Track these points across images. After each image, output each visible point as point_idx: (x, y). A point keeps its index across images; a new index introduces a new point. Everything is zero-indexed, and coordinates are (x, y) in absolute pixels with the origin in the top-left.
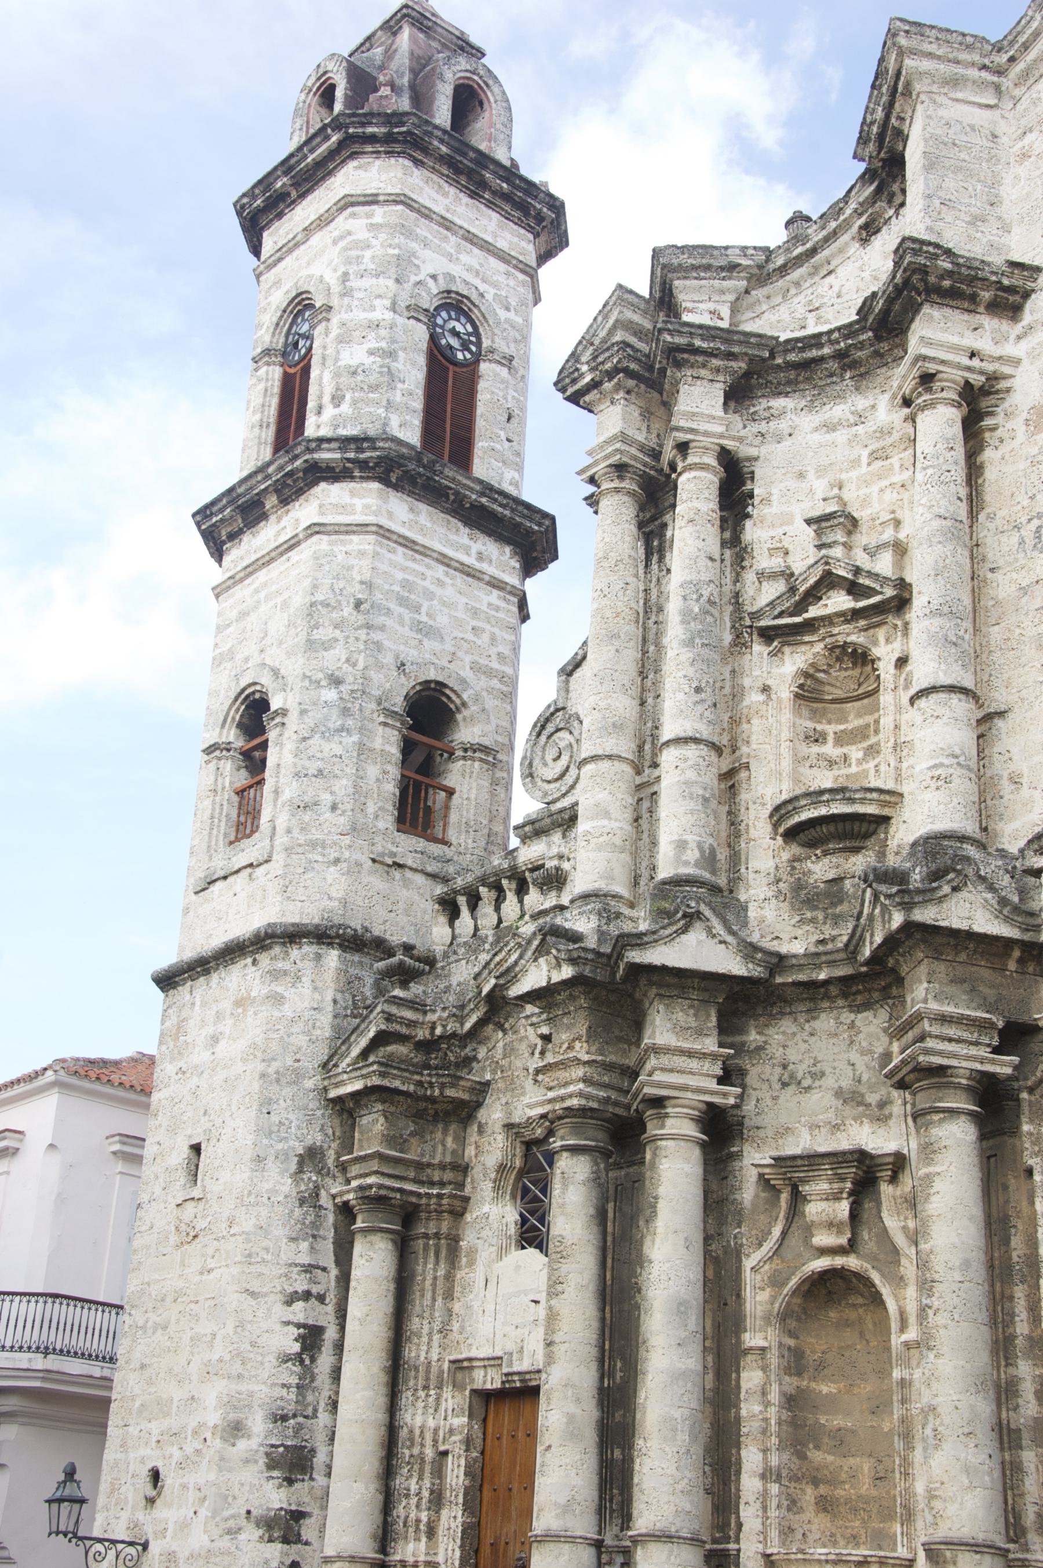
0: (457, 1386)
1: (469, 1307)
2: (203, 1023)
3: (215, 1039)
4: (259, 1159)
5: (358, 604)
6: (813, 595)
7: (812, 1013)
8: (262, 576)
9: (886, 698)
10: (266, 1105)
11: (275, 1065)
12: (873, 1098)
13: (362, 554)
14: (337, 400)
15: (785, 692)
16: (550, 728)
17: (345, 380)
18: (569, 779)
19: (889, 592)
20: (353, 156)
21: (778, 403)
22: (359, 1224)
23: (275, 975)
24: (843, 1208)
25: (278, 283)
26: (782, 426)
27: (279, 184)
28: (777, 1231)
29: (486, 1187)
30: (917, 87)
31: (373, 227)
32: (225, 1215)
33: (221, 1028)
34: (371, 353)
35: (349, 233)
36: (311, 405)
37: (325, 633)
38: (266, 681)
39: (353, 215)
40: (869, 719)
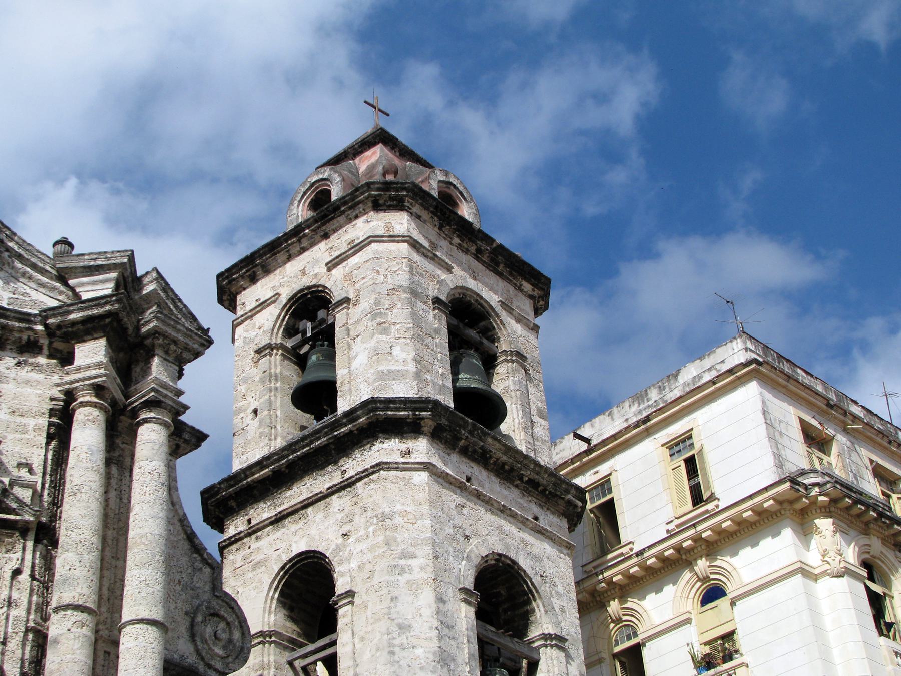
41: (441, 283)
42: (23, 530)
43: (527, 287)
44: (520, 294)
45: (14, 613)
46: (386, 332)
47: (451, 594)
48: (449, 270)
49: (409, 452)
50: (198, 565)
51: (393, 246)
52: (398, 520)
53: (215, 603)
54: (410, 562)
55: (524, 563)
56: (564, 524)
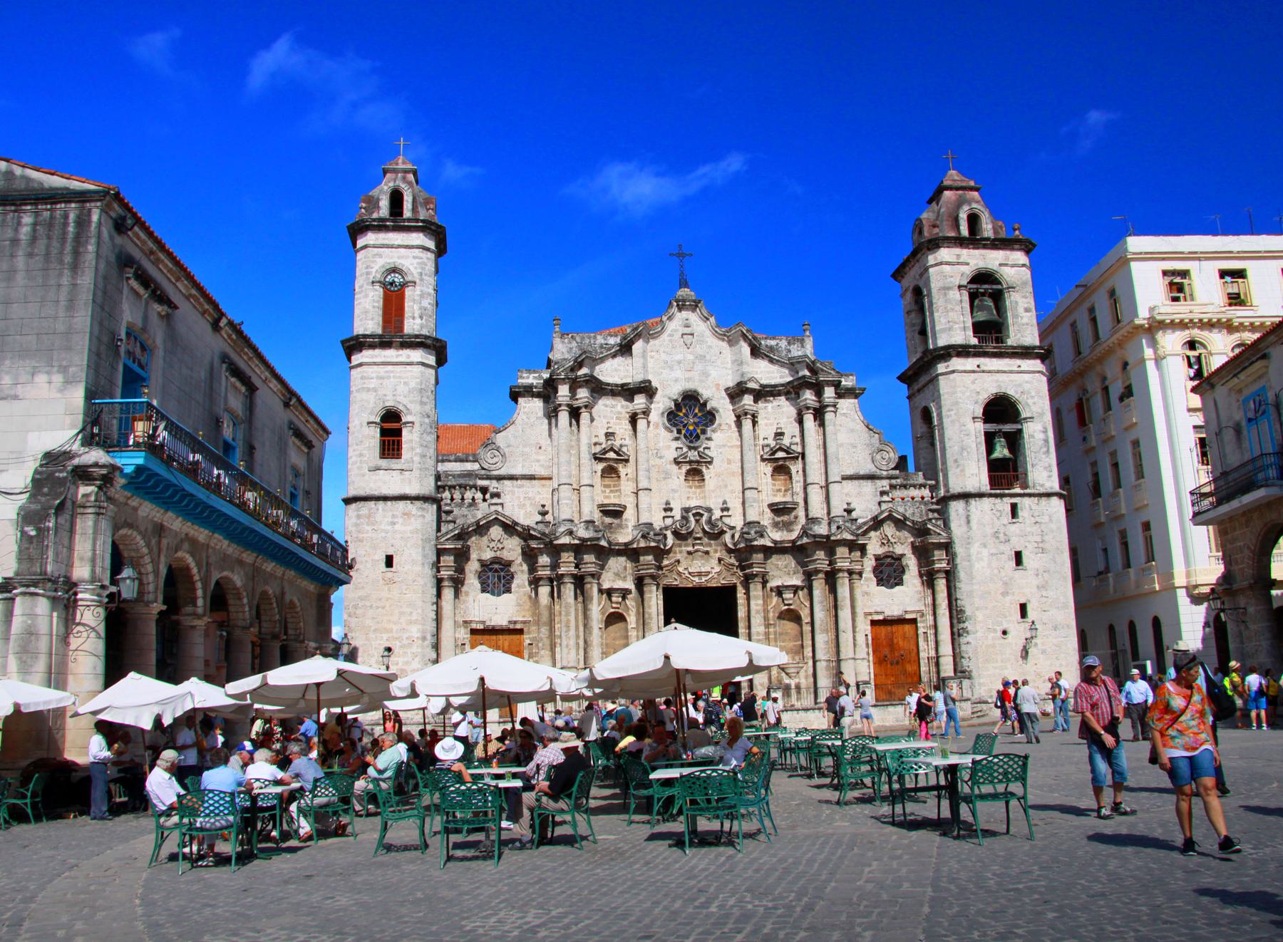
0: (466, 627)
2: (384, 516)
3: (393, 524)
4: (423, 564)
8: (390, 368)
9: (622, 482)
10: (423, 548)
15: (599, 473)
16: (490, 447)
22: (446, 583)
23: (423, 509)
24: (620, 599)
25: (380, 256)
37: (425, 399)
38: (401, 408)
43: (1017, 247)
48: (967, 264)
51: (937, 268)
52: (946, 396)
53: (881, 447)
54: (952, 413)
55: (1011, 392)
56: (1038, 361)
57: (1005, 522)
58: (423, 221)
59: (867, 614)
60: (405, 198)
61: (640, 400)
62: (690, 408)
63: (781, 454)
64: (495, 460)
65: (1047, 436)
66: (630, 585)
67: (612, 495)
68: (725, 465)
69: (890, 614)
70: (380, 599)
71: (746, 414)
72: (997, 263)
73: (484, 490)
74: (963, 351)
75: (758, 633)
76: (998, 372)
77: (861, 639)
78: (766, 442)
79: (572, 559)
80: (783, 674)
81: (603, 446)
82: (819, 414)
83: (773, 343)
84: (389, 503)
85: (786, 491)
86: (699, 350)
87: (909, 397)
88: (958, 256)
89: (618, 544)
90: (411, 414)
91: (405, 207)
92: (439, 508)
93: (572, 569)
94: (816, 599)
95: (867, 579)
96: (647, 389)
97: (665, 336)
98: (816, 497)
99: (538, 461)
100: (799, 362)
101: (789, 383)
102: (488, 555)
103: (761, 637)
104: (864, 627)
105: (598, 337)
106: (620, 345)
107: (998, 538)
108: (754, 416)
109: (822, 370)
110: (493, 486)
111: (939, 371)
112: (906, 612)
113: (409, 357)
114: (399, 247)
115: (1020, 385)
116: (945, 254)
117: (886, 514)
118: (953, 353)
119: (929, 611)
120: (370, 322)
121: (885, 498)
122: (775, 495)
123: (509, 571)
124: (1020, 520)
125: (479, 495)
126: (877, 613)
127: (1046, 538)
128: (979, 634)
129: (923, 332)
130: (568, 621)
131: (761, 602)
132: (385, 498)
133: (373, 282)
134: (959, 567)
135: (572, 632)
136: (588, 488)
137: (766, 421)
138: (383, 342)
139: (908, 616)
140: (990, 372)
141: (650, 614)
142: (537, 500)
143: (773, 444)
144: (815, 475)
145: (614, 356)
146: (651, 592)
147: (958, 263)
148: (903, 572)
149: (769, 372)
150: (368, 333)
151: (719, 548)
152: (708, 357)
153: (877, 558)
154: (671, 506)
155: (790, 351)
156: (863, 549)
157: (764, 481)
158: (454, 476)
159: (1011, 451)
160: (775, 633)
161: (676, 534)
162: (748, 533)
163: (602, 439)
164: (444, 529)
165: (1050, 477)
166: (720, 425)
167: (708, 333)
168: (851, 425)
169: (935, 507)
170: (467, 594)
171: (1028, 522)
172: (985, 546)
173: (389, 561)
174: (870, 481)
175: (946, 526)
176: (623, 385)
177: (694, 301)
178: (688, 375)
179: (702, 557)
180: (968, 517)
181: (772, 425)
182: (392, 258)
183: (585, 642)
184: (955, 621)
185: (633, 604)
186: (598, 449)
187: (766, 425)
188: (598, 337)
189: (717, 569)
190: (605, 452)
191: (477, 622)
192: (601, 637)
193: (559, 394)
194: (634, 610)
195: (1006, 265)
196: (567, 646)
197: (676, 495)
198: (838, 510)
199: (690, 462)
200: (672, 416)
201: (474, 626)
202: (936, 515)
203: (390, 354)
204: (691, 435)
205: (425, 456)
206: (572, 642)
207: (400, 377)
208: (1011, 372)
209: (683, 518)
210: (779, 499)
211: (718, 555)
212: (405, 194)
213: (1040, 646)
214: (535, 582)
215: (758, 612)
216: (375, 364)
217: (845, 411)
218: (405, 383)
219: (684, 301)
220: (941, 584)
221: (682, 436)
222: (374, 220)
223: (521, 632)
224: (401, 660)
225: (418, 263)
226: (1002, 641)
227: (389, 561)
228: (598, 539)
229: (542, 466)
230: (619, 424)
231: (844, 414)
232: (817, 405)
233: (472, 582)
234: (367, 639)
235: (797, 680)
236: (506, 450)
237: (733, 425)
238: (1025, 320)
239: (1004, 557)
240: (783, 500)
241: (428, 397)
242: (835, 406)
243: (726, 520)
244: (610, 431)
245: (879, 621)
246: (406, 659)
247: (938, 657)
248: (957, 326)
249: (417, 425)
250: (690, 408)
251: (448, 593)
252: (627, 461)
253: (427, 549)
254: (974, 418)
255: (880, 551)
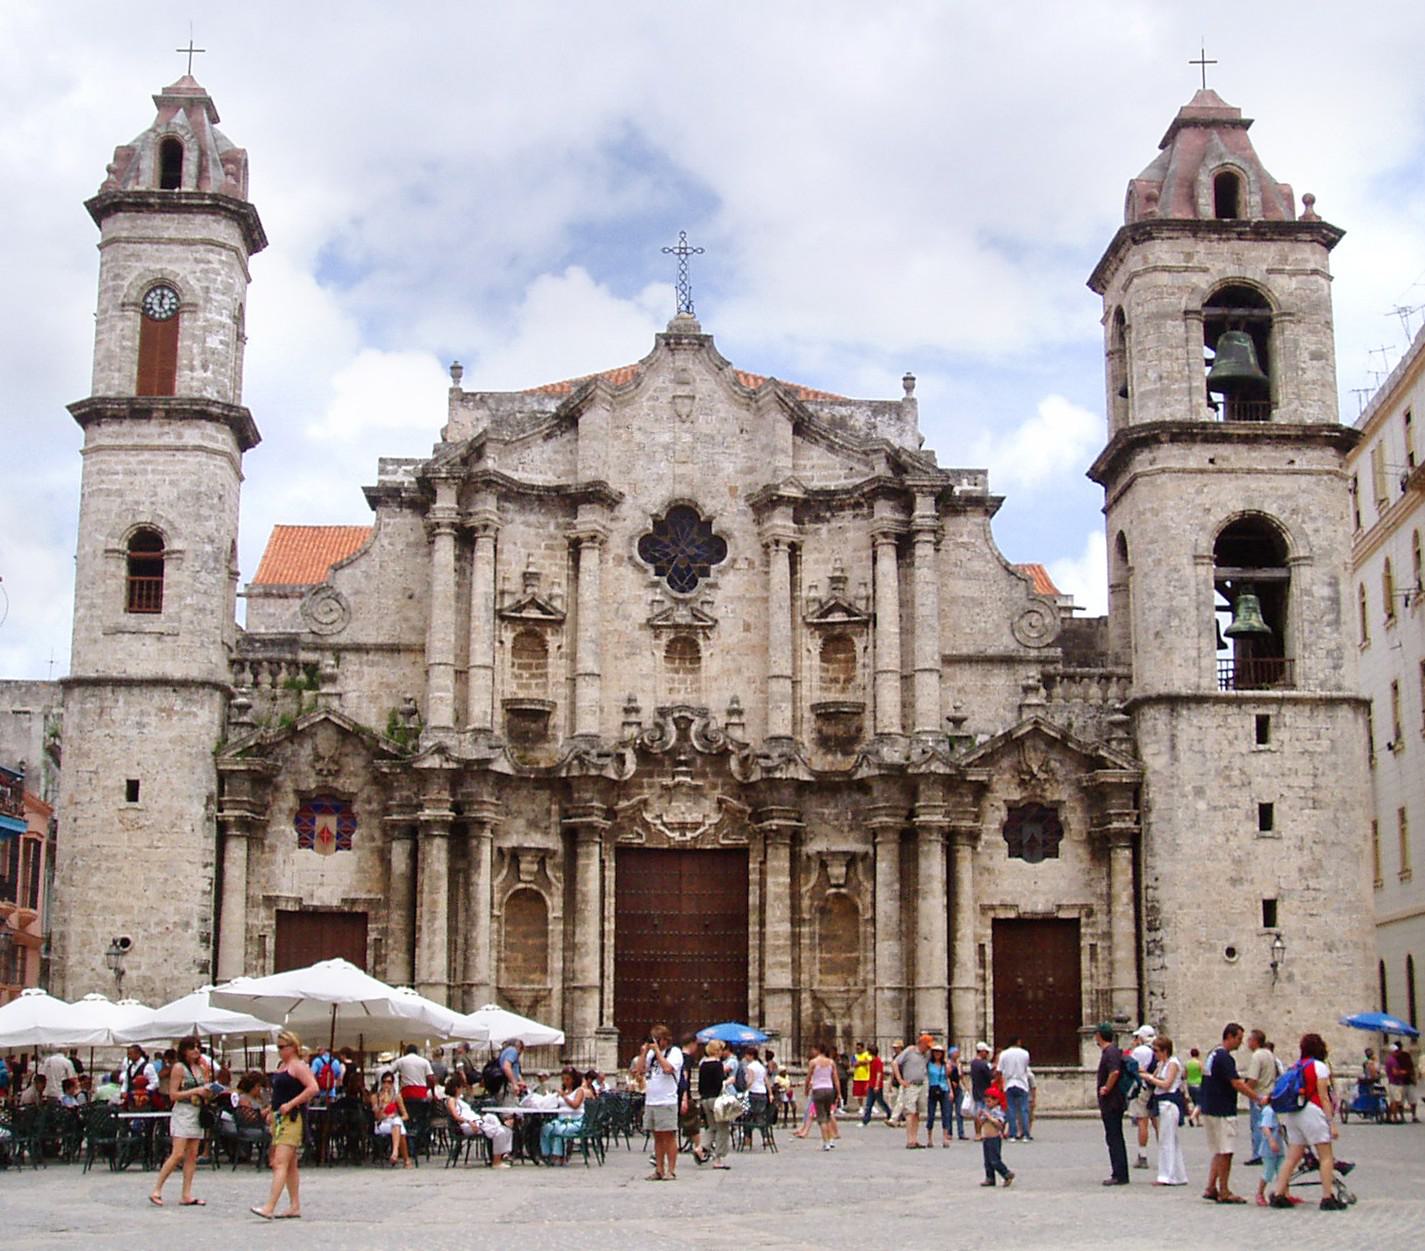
0: (269, 907)
1: (272, 872)
3: (140, 725)
5: (220, 497)
6: (524, 607)
7: (518, 788)
8: (146, 456)
9: (550, 660)
11: (194, 751)
12: (543, 825)
13: (222, 468)
14: (205, 368)
15: (508, 645)
16: (324, 595)
17: (208, 356)
18: (339, 626)
19: (559, 617)
20: (213, 214)
21: (507, 505)
24: (535, 867)
25: (138, 257)
26: (509, 517)
27: (152, 200)
28: (505, 872)
29: (283, 817)
30: (597, 400)
31: (221, 262)
32: (167, 821)
33: (145, 720)
34: (221, 342)
35: (209, 262)
36: (182, 361)
37: (205, 511)
38: (162, 525)
39: (212, 251)
40: (534, 662)
41: (1194, 290)
42: (866, 623)
44: (1299, 244)
45: (868, 670)
46: (1143, 358)
47: (1186, 561)
48: (1205, 270)
49: (1154, 459)
50: (1015, 581)
52: (1148, 515)
53: (1029, 606)
55: (1271, 509)
56: (1331, 452)
57: (1243, 747)
58: (213, 196)
59: (984, 909)
60: (186, 154)
61: (589, 519)
62: (683, 530)
63: (838, 617)
64: (334, 616)
65: (1337, 592)
66: (554, 843)
67: (533, 682)
68: (739, 634)
69: (1029, 910)
70: (115, 855)
71: (777, 543)
72: (1265, 267)
73: (312, 669)
74: (1186, 433)
75: (777, 935)
76: (1249, 472)
77: (966, 951)
78: (813, 594)
79: (445, 795)
80: (824, 1010)
81: (519, 596)
82: (904, 545)
83: (844, 411)
84: (136, 691)
85: (848, 680)
86: (704, 425)
87: (1105, 511)
88: (1189, 256)
89: (538, 771)
90: (179, 535)
91: (184, 169)
92: (229, 696)
93: (449, 815)
94: (880, 878)
95: (988, 844)
96: (598, 495)
97: (644, 403)
98: (889, 696)
99: (406, 620)
100: (875, 451)
101: (857, 487)
102: (311, 783)
103: (781, 942)
104: (974, 931)
105: (528, 400)
106: (556, 416)
107: (1228, 778)
108: (794, 549)
109: (914, 467)
110: (327, 663)
111: (1139, 470)
112: (1059, 907)
113: (180, 436)
114: (171, 241)
115: (1289, 497)
116: (1162, 251)
117: (1029, 728)
118: (1164, 437)
119: (1098, 905)
120: (116, 375)
121: (1033, 700)
122: (827, 689)
123: (349, 811)
124: (1273, 745)
125: (302, 677)
126: (1004, 906)
127: (1321, 781)
128: (1183, 953)
129: (1124, 393)
130: (434, 903)
131: (788, 880)
132: (129, 683)
133: (123, 305)
134: (1153, 828)
135: (442, 922)
136: (482, 671)
137: (816, 555)
138: (137, 412)
139: (1062, 915)
140: (1232, 471)
141: (584, 895)
142: (402, 687)
143: (822, 593)
144: (889, 657)
145: (548, 437)
146: (588, 855)
147: (1187, 269)
148: (1060, 834)
149: (825, 467)
150: (111, 394)
151: (720, 781)
152: (719, 438)
153: (1012, 808)
154: (639, 704)
155: (875, 427)
156: (982, 789)
157: (806, 663)
158: (264, 643)
159: (1266, 622)
160: (812, 936)
161: (643, 753)
162: (767, 757)
163: (514, 584)
164: (233, 739)
165: (1336, 667)
166: (734, 561)
167: (720, 394)
168: (977, 565)
169: (1120, 717)
170: (273, 849)
171: (1286, 748)
172: (1199, 792)
173: (133, 790)
174: (1004, 667)
175: (1136, 754)
176: (558, 489)
177: (697, 337)
178: (681, 470)
179: (687, 795)
180: (1173, 737)
181: (826, 561)
182: (159, 260)
183: (466, 940)
184: (1145, 926)
185: (560, 874)
186: (508, 602)
187: (816, 562)
188: (528, 400)
189: (715, 818)
190: (520, 607)
191: (288, 899)
192: (499, 932)
193: (438, 505)
194: (561, 886)
195: (1281, 272)
196: (430, 946)
197: (648, 684)
198: (930, 715)
199: (676, 626)
200: (650, 546)
201: (282, 906)
202: (1121, 734)
203: (150, 432)
204: (682, 579)
205: (202, 610)
206: (441, 938)
207: (163, 472)
208: (1274, 472)
209: (657, 725)
210: (833, 696)
211: (717, 793)
212: (186, 146)
213: (1298, 978)
214: (390, 832)
215: (778, 897)
216: (120, 448)
217: (965, 539)
218: (172, 483)
219: (678, 338)
220: (1123, 857)
221: (664, 580)
222: (128, 195)
223: (362, 919)
224: (144, 961)
225: (205, 271)
226: (1224, 967)
227: (133, 790)
228: (489, 761)
229: (413, 628)
230: (553, 557)
231: (964, 545)
232: (902, 530)
233: (284, 829)
234: (90, 925)
235: (847, 1021)
236: (351, 599)
237: (757, 563)
238: (1310, 375)
239: (1239, 814)
240: (841, 698)
241: (212, 507)
242: (935, 532)
243: (737, 734)
244: (531, 570)
245: (1008, 920)
246: (154, 960)
247: (1112, 990)
248: (1176, 386)
249: (190, 556)
250: (683, 530)
251: (237, 850)
252: (561, 622)
253: (199, 770)
254: (1195, 557)
255: (1016, 795)
